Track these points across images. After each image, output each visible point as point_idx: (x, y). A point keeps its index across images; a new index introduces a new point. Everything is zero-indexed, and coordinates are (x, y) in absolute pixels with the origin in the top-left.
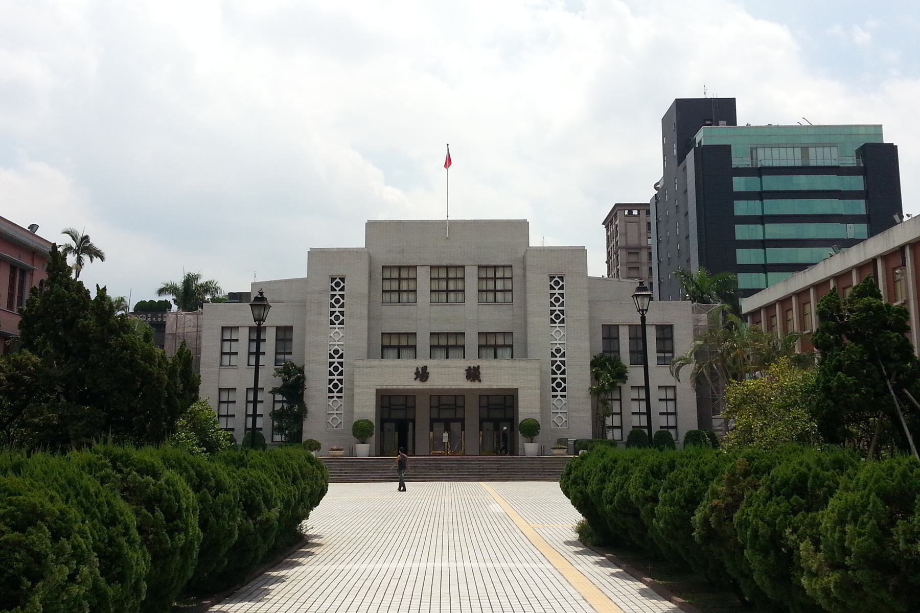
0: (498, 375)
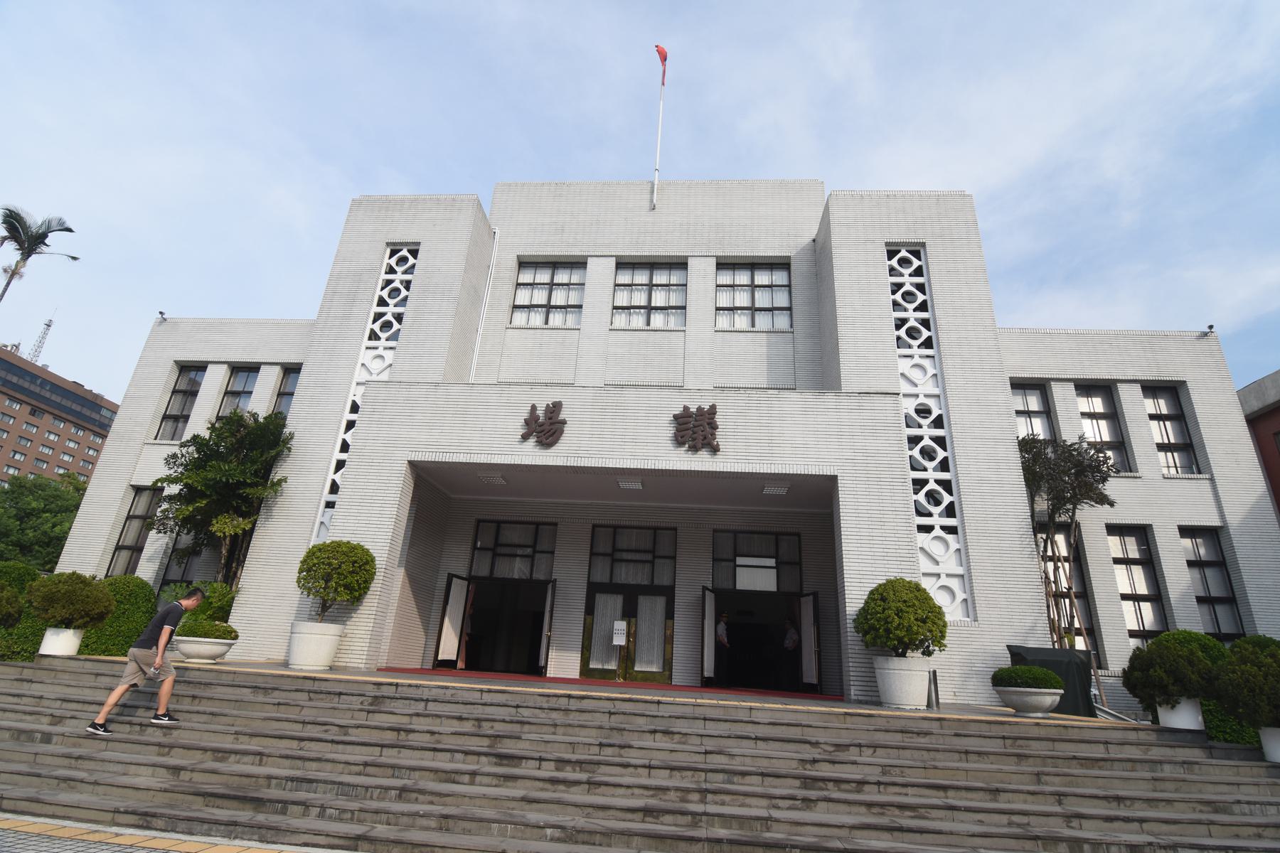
0: (768, 440)
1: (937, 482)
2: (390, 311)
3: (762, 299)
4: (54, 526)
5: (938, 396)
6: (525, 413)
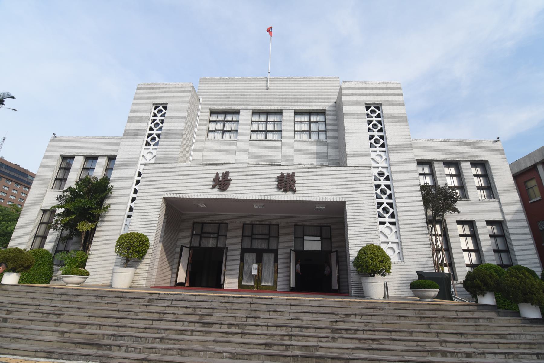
1: (387, 203)
2: (155, 133)
3: (314, 127)
4: (7, 227)
5: (387, 168)
6: (213, 176)
